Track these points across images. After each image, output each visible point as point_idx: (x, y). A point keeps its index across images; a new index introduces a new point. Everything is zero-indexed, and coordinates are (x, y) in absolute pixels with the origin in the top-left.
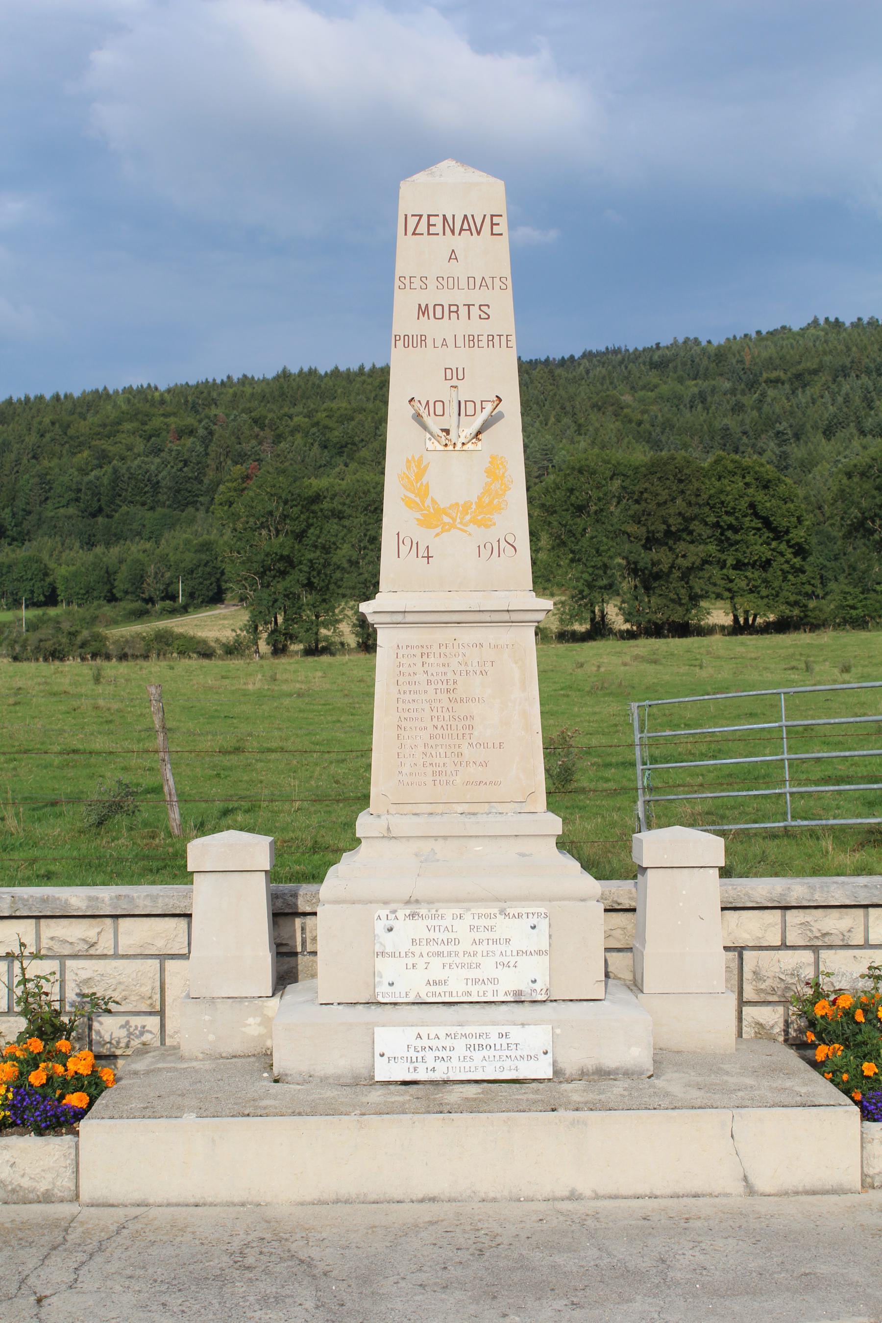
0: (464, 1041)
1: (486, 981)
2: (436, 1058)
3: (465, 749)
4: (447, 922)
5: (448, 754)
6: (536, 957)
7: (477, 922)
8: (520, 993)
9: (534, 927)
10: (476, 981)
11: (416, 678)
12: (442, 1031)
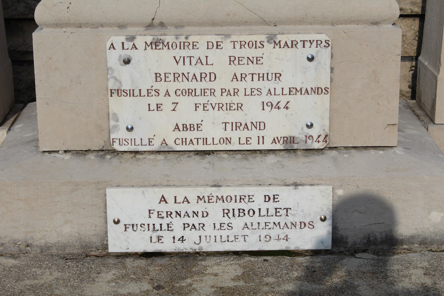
0: (220, 206)
1: (249, 125)
2: (185, 226)
4: (201, 52)
6: (313, 97)
7: (238, 52)
8: (291, 140)
9: (311, 59)
10: (237, 126)
12: (192, 193)
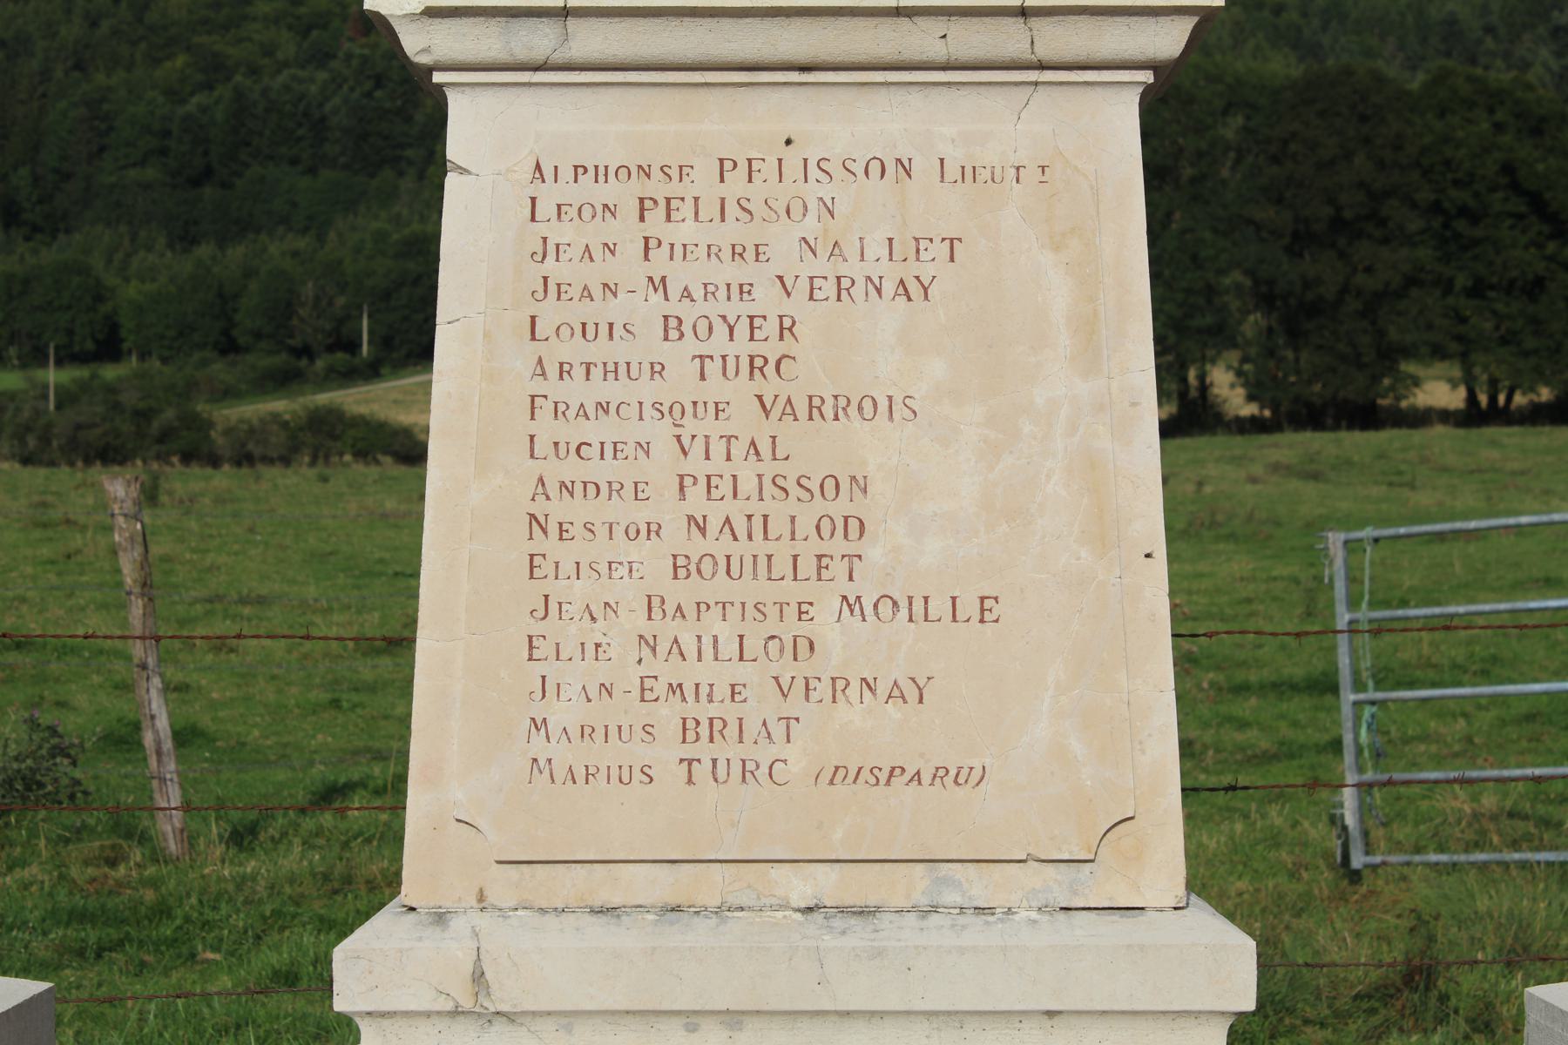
3: (827, 625)
5: (753, 646)
11: (614, 310)
